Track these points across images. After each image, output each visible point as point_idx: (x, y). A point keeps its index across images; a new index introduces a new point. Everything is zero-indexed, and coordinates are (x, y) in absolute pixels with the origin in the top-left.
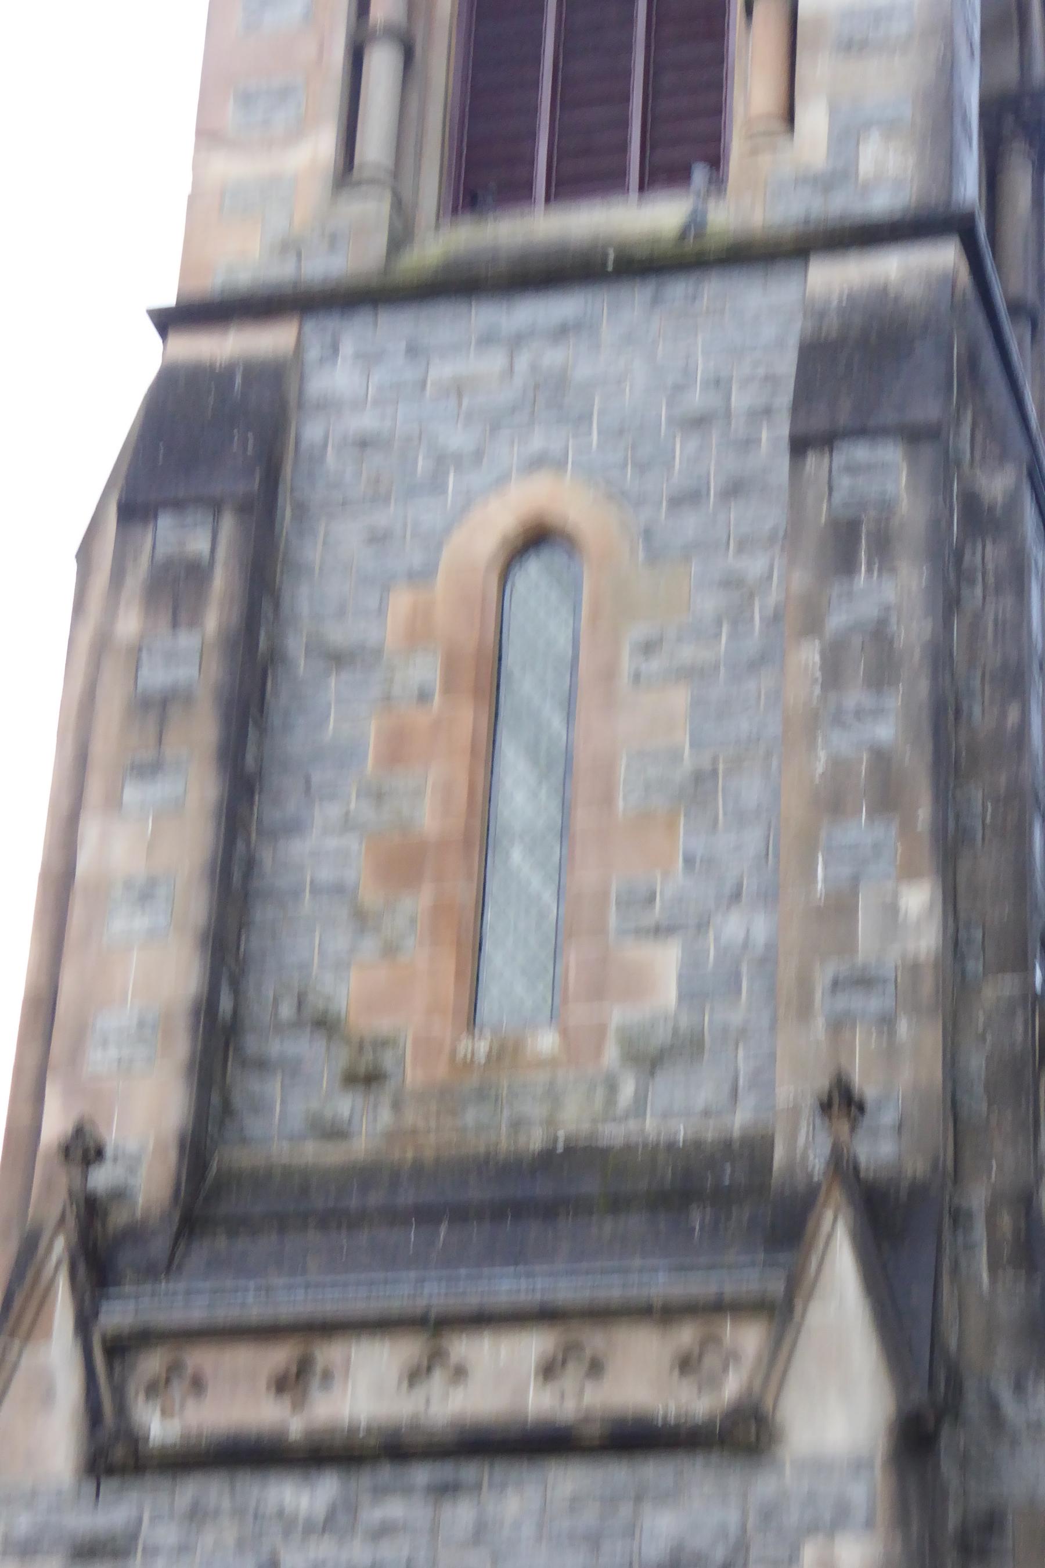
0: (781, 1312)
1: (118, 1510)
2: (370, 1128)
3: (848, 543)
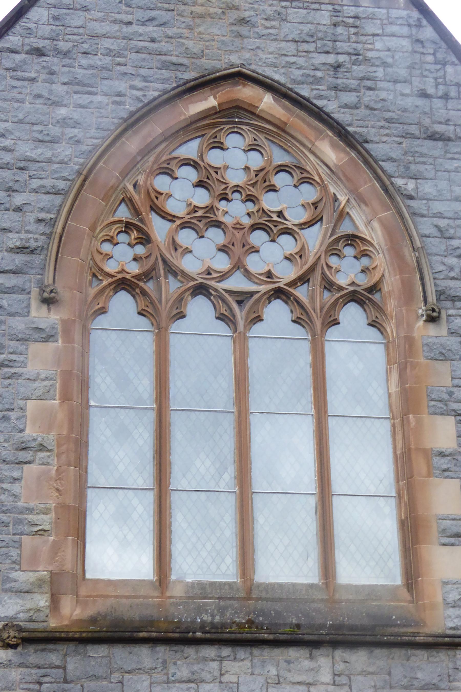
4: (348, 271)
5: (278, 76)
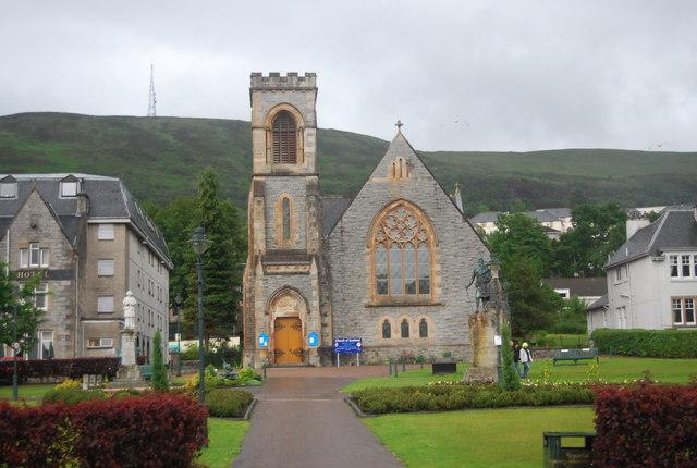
0: (310, 265)
1: (269, 277)
2: (277, 247)
3: (310, 205)
4: (422, 237)
5: (409, 199)
